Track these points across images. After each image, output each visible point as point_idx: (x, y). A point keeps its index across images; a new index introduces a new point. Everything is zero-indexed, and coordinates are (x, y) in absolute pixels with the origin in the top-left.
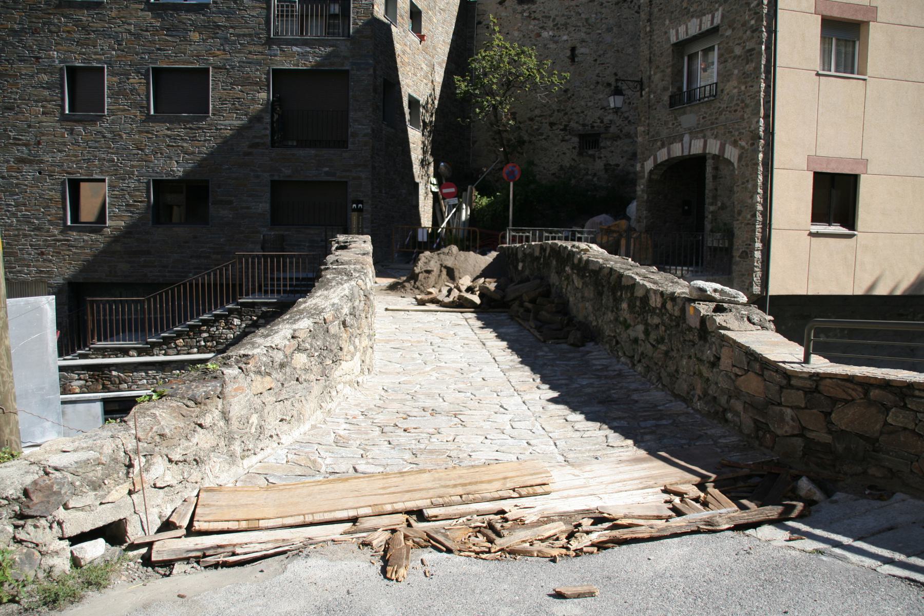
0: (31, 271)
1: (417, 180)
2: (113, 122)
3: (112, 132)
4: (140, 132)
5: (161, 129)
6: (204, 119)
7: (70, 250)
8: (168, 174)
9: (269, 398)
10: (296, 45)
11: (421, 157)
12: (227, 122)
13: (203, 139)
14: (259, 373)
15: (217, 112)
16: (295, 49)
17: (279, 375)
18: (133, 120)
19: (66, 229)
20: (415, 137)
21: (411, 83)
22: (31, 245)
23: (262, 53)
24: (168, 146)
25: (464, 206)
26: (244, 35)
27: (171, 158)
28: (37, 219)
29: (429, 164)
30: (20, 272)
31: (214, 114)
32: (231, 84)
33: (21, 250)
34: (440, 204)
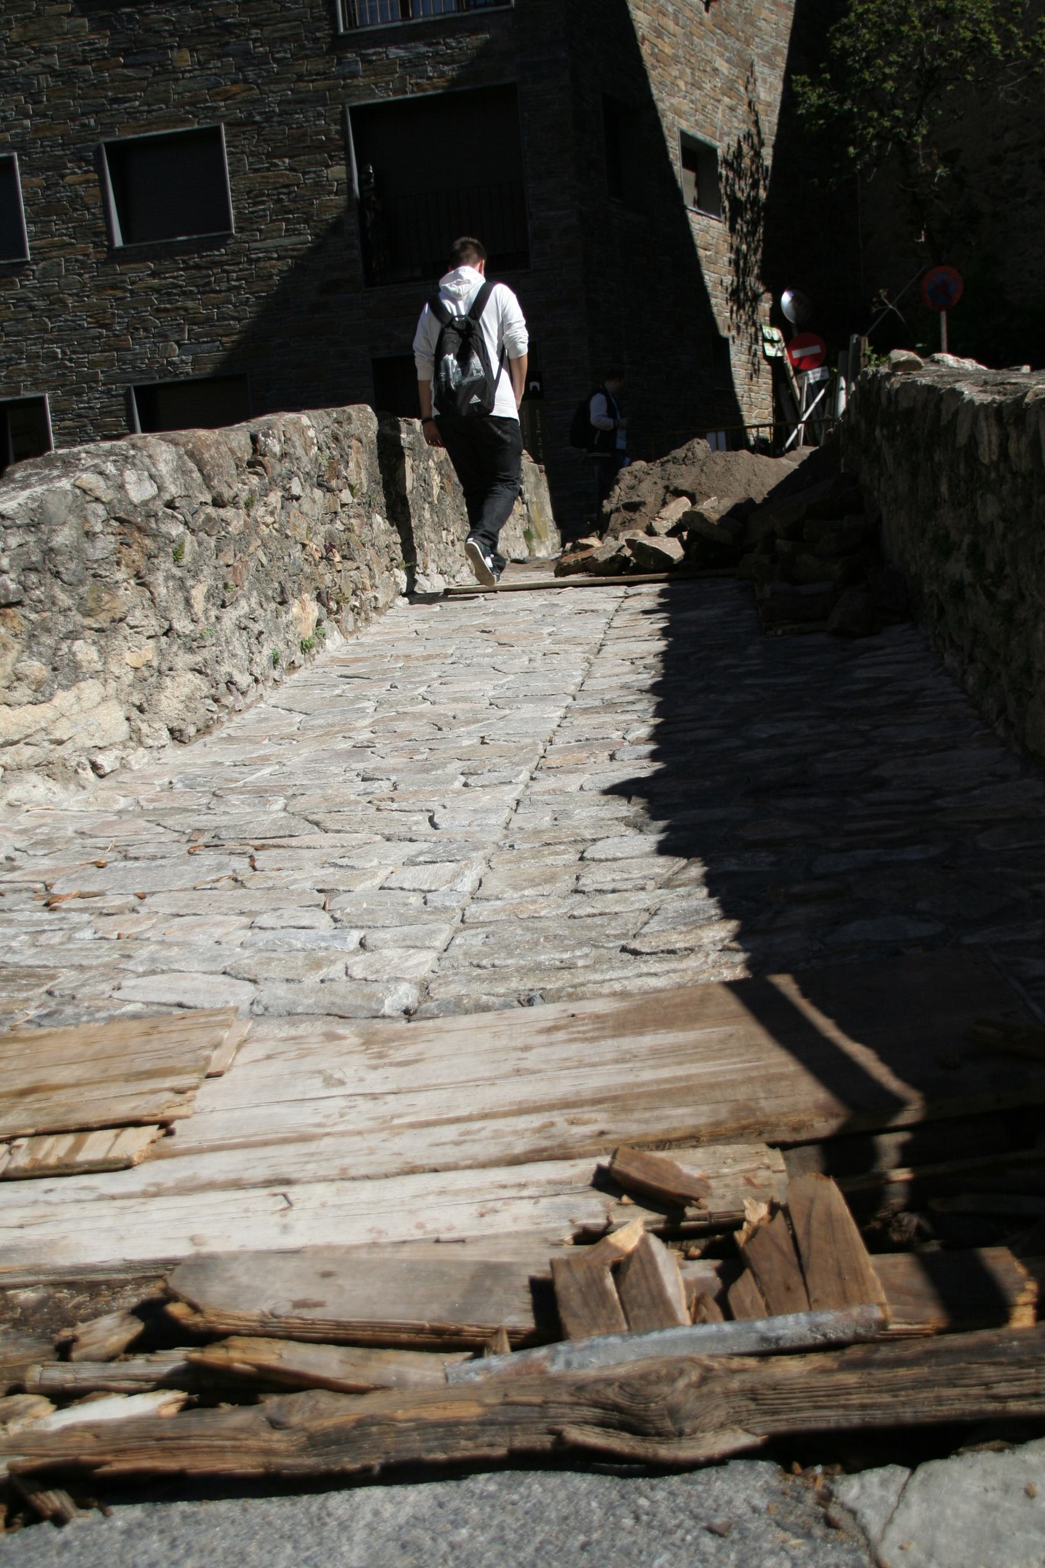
1: (724, 333)
2: (45, 275)
3: (44, 295)
4: (99, 289)
5: (139, 275)
6: (221, 242)
8: (163, 372)
10: (396, 43)
11: (728, 280)
12: (269, 243)
13: (224, 286)
15: (247, 222)
16: (394, 52)
18: (83, 265)
20: (709, 233)
21: (686, 106)
23: (325, 75)
24: (158, 310)
25: (843, 383)
26: (284, 39)
27: (165, 337)
29: (756, 298)
31: (241, 230)
32: (269, 156)
34: (790, 386)
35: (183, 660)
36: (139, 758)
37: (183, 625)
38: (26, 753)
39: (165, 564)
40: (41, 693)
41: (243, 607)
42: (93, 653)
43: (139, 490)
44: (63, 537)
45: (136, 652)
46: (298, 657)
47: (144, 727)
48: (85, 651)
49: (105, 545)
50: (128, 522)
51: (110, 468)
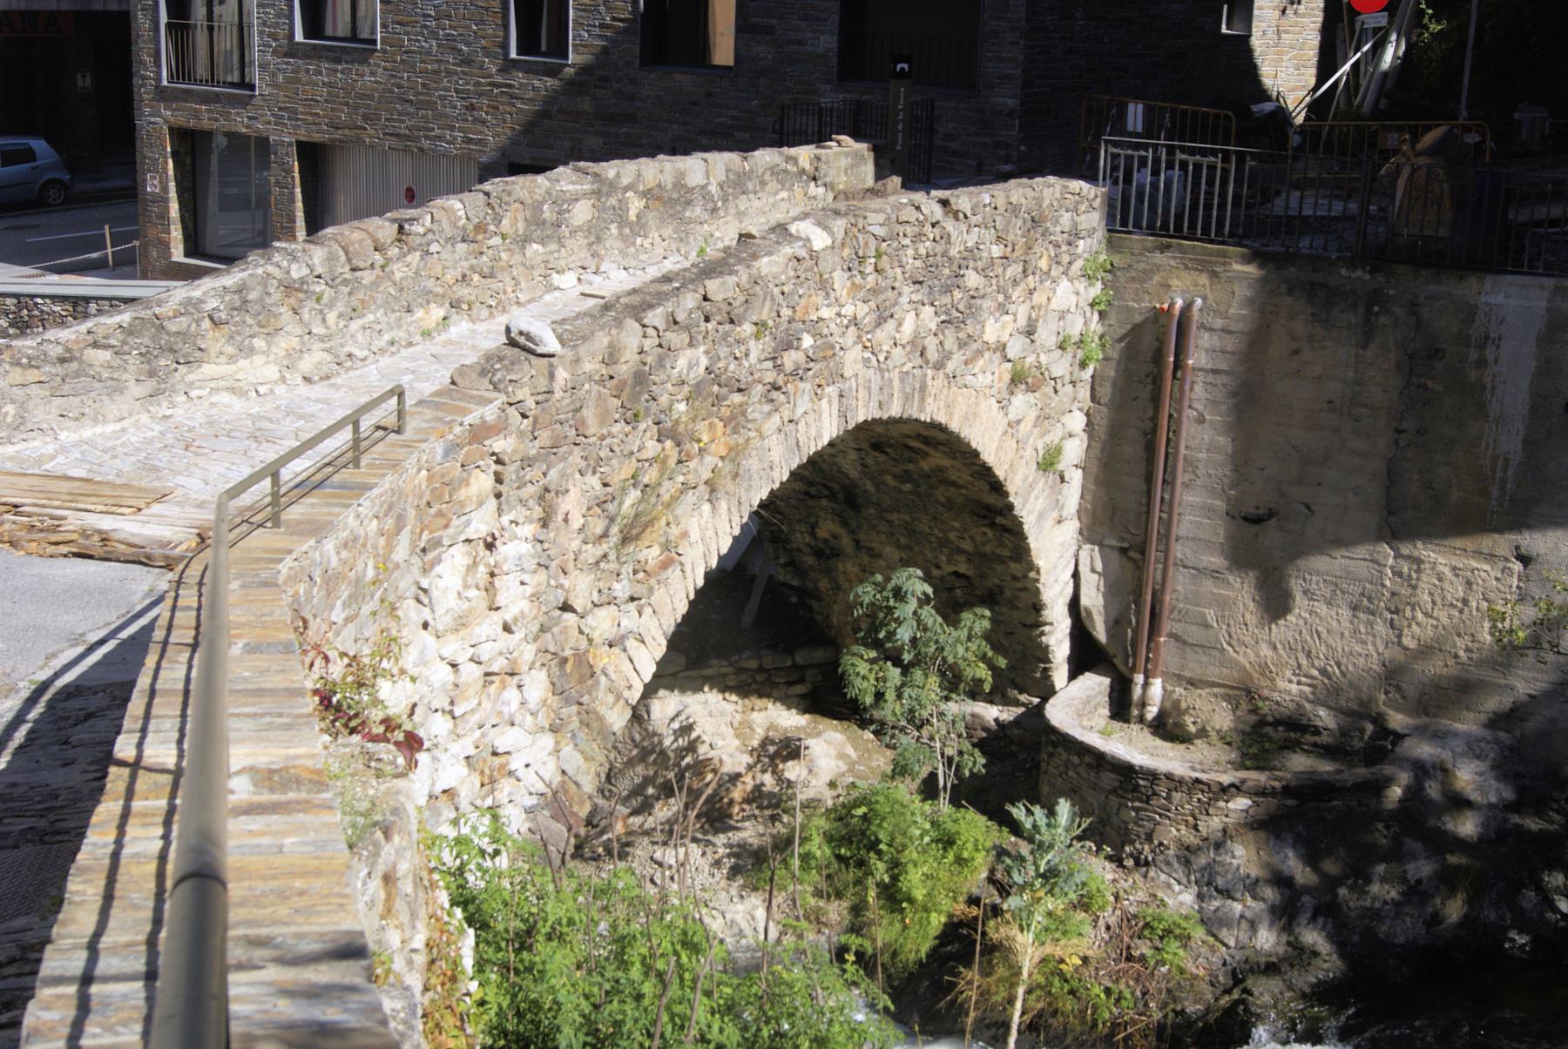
0: (455, 138)
7: (513, 105)
9: (35, 390)
14: (19, 364)
17: (59, 369)
19: (508, 66)
22: (457, 91)
25: (1394, 37)
28: (467, 44)
30: (439, 138)
33: (443, 98)
35: (318, 345)
36: (280, 390)
37: (318, 329)
38: (222, 383)
39: (311, 304)
40: (232, 359)
41: (370, 317)
42: (263, 344)
43: (298, 271)
44: (253, 296)
45: (283, 344)
46: (418, 337)
47: (288, 376)
48: (259, 343)
49: (277, 296)
50: (289, 288)
51: (285, 264)
